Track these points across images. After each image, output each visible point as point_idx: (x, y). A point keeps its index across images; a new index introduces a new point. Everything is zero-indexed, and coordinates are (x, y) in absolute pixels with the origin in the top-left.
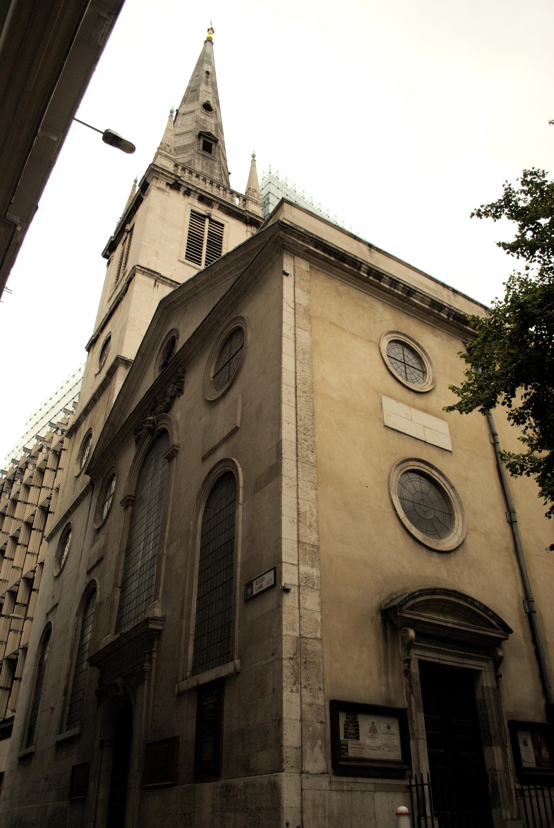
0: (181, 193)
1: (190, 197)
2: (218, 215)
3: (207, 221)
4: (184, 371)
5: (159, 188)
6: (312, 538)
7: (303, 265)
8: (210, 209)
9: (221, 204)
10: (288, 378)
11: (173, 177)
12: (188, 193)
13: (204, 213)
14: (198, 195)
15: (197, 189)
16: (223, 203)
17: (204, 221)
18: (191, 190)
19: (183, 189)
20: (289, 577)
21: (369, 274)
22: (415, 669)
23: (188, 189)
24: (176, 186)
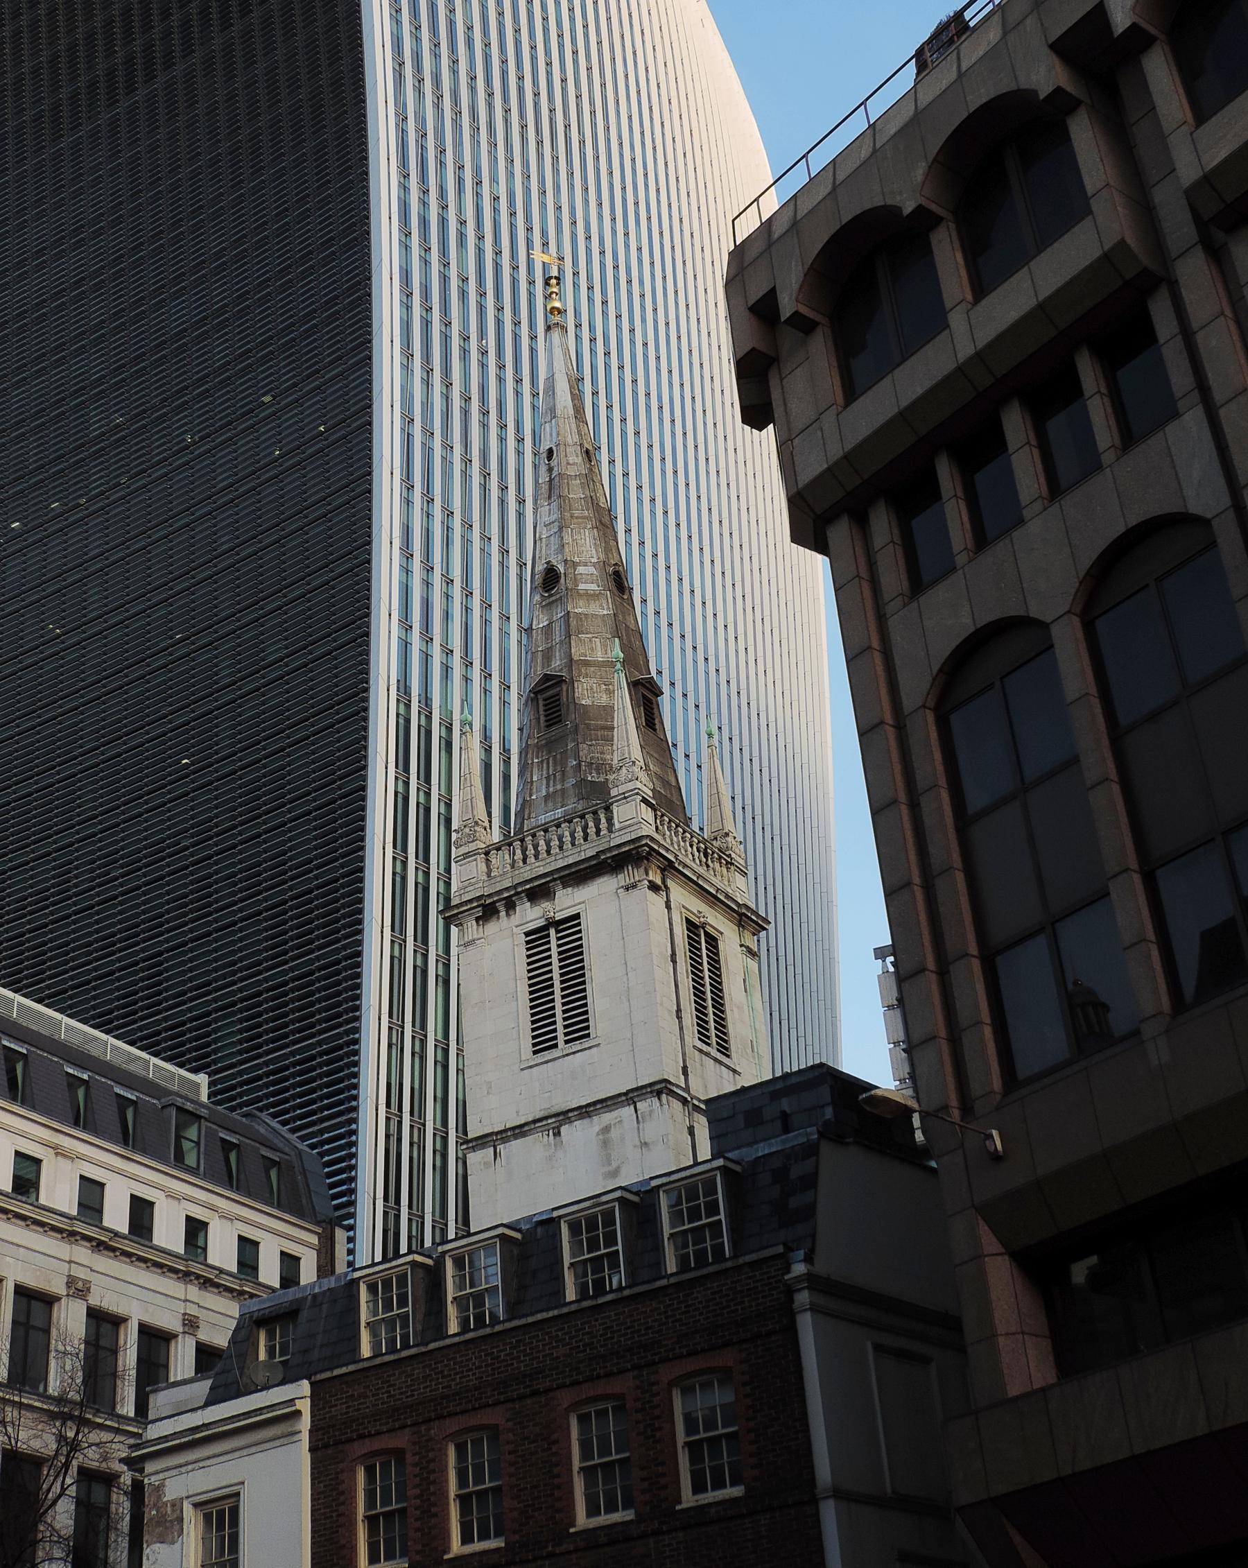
0: (503, 914)
2: (565, 901)
3: (552, 931)
8: (546, 905)
9: (560, 878)
12: (510, 906)
13: (541, 923)
15: (515, 887)
17: (548, 936)
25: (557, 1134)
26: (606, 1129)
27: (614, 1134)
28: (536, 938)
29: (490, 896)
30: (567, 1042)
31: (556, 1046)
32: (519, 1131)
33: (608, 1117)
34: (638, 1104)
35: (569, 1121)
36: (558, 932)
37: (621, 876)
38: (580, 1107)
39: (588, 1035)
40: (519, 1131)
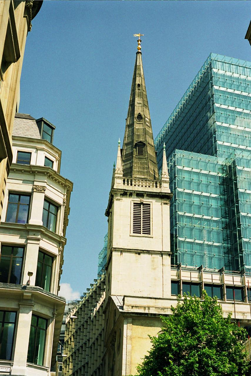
0: (128, 196)
1: (133, 196)
2: (146, 200)
3: (142, 205)
5: (117, 200)
8: (142, 199)
11: (123, 191)
12: (131, 195)
13: (139, 202)
14: (135, 194)
15: (135, 191)
16: (148, 193)
17: (141, 206)
18: (132, 193)
19: (128, 194)
23: (131, 193)
24: (125, 193)
26: (154, 258)
27: (155, 259)
29: (127, 190)
30: (143, 233)
31: (140, 233)
32: (129, 251)
33: (154, 256)
34: (163, 256)
35: (144, 253)
36: (143, 206)
37: (163, 200)
38: (148, 251)
40: (129, 251)
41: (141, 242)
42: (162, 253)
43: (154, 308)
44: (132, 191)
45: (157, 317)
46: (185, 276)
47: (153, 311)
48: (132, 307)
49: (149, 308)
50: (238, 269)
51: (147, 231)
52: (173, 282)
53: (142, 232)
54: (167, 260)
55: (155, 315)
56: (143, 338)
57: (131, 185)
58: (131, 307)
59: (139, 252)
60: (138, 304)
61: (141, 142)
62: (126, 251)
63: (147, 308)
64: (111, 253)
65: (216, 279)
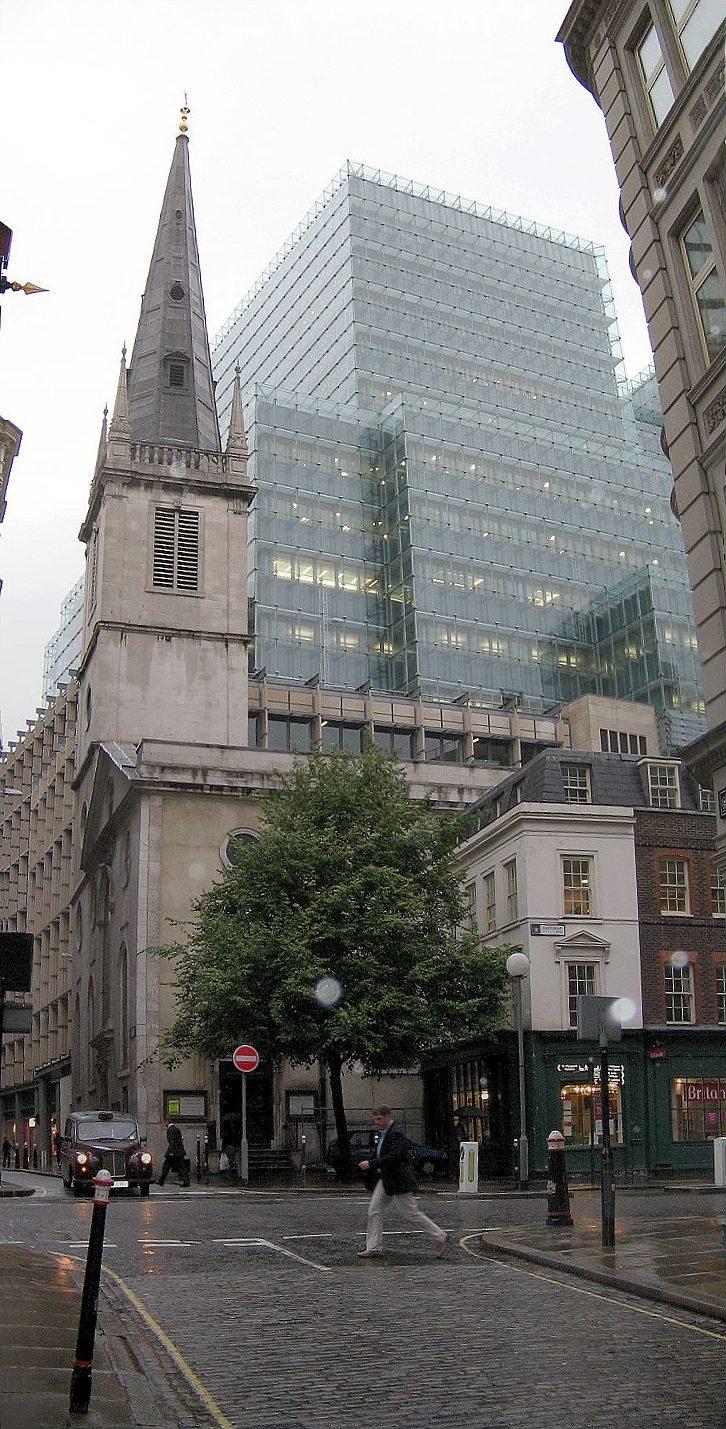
0: (142, 488)
2: (190, 501)
3: (177, 516)
4: (115, 836)
6: (156, 1007)
7: (157, 801)
10: (142, 904)
17: (173, 516)
20: (141, 1031)
21: (211, 789)
22: (217, 1069)
24: (134, 481)
25: (169, 640)
28: (163, 514)
30: (179, 587)
31: (172, 586)
32: (143, 629)
35: (180, 636)
39: (196, 589)
40: (143, 629)
41: (171, 609)
42: (225, 638)
43: (219, 774)
44: (154, 476)
45: (224, 793)
46: (274, 703)
47: (215, 779)
48: (163, 768)
49: (205, 771)
50: (401, 685)
51: (190, 581)
52: (252, 714)
53: (175, 584)
54: (239, 657)
55: (220, 788)
56: (189, 847)
57: (151, 460)
58: (158, 770)
59: (169, 634)
60: (178, 761)
61: (178, 354)
62: (133, 631)
63: (200, 773)
64: (97, 634)
65: (352, 709)
